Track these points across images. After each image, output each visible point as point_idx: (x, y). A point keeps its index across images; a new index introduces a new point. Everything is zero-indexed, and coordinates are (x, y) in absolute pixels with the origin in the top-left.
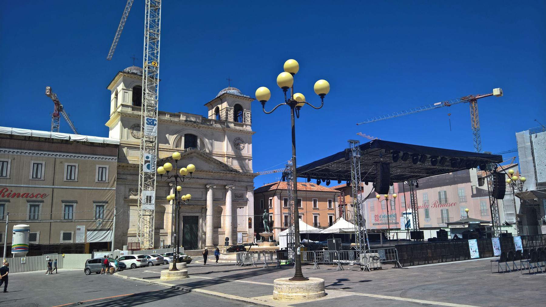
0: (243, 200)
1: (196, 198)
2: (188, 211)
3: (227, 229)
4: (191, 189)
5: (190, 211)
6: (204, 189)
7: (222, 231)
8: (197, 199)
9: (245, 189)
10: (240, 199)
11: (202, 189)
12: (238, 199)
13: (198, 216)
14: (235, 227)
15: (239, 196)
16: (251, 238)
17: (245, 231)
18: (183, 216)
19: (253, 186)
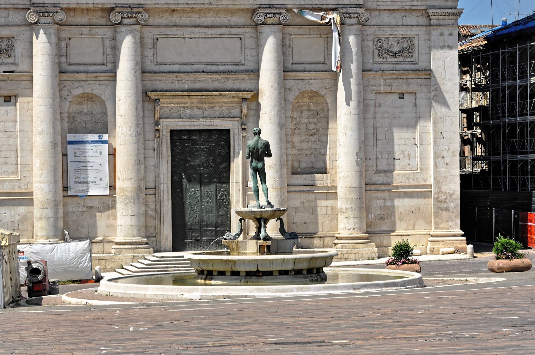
0: (414, 63)
1: (217, 64)
2: (188, 112)
3: (341, 175)
4: (197, 30)
5: (198, 112)
6: (248, 29)
7: (328, 183)
8: (221, 68)
9: (422, 20)
10: (401, 59)
11: (241, 30)
12: (393, 60)
13: (228, 131)
14: (382, 166)
15: (397, 49)
16: (447, 209)
17: (422, 183)
18: (172, 132)
19: (455, 7)
